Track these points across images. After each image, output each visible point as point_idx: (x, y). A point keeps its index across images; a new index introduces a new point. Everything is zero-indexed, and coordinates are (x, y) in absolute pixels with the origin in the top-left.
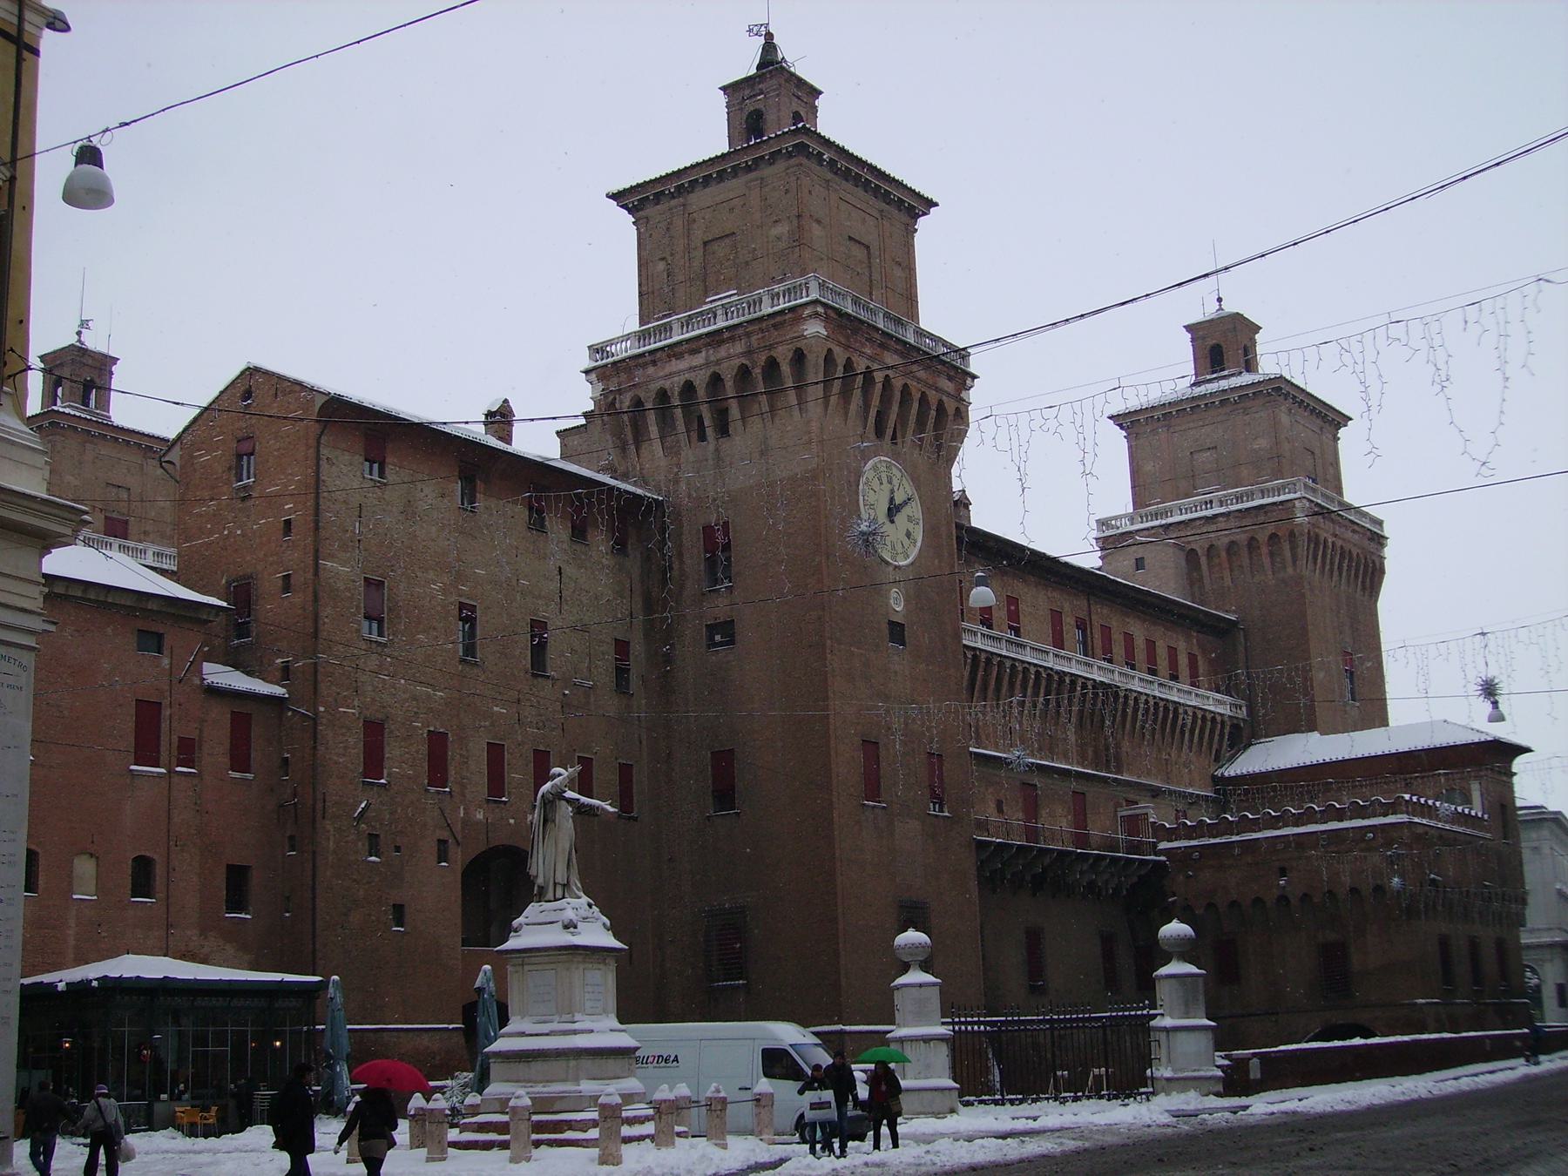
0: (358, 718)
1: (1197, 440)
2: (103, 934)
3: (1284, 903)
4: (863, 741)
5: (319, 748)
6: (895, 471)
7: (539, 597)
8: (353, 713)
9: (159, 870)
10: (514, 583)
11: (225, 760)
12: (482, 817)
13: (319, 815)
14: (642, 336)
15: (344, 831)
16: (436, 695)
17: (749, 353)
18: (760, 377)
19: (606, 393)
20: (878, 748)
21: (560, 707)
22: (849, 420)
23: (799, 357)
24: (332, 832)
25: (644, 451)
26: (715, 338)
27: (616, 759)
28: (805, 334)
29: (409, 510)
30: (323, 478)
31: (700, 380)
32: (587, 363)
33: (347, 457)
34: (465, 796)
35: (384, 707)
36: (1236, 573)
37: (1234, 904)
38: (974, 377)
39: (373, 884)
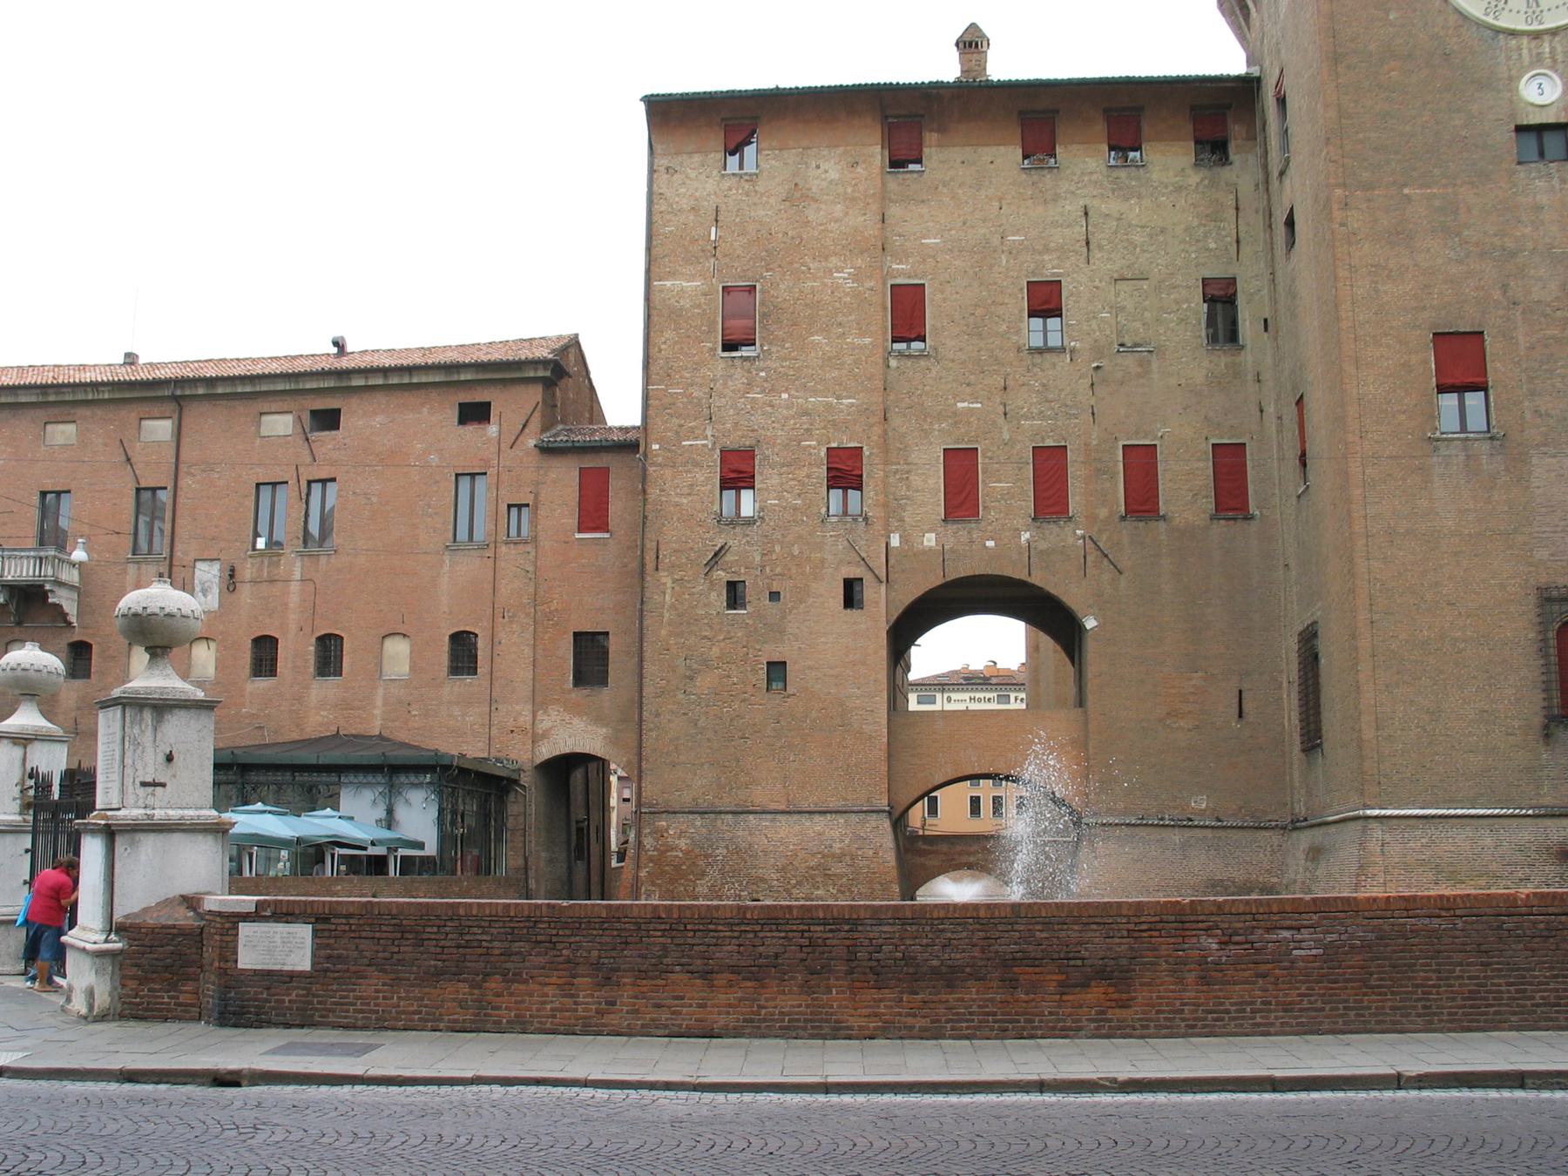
0: (713, 449)
2: (414, 713)
5: (649, 491)
7: (1047, 250)
8: (703, 445)
9: (482, 644)
10: (996, 241)
11: (573, 521)
12: (933, 543)
13: (650, 566)
15: (689, 582)
16: (841, 404)
20: (1483, 341)
24: (669, 584)
25: (1252, 23)
29: (797, 196)
30: (661, 191)
33: (697, 158)
34: (902, 520)
35: (753, 431)
39: (735, 639)
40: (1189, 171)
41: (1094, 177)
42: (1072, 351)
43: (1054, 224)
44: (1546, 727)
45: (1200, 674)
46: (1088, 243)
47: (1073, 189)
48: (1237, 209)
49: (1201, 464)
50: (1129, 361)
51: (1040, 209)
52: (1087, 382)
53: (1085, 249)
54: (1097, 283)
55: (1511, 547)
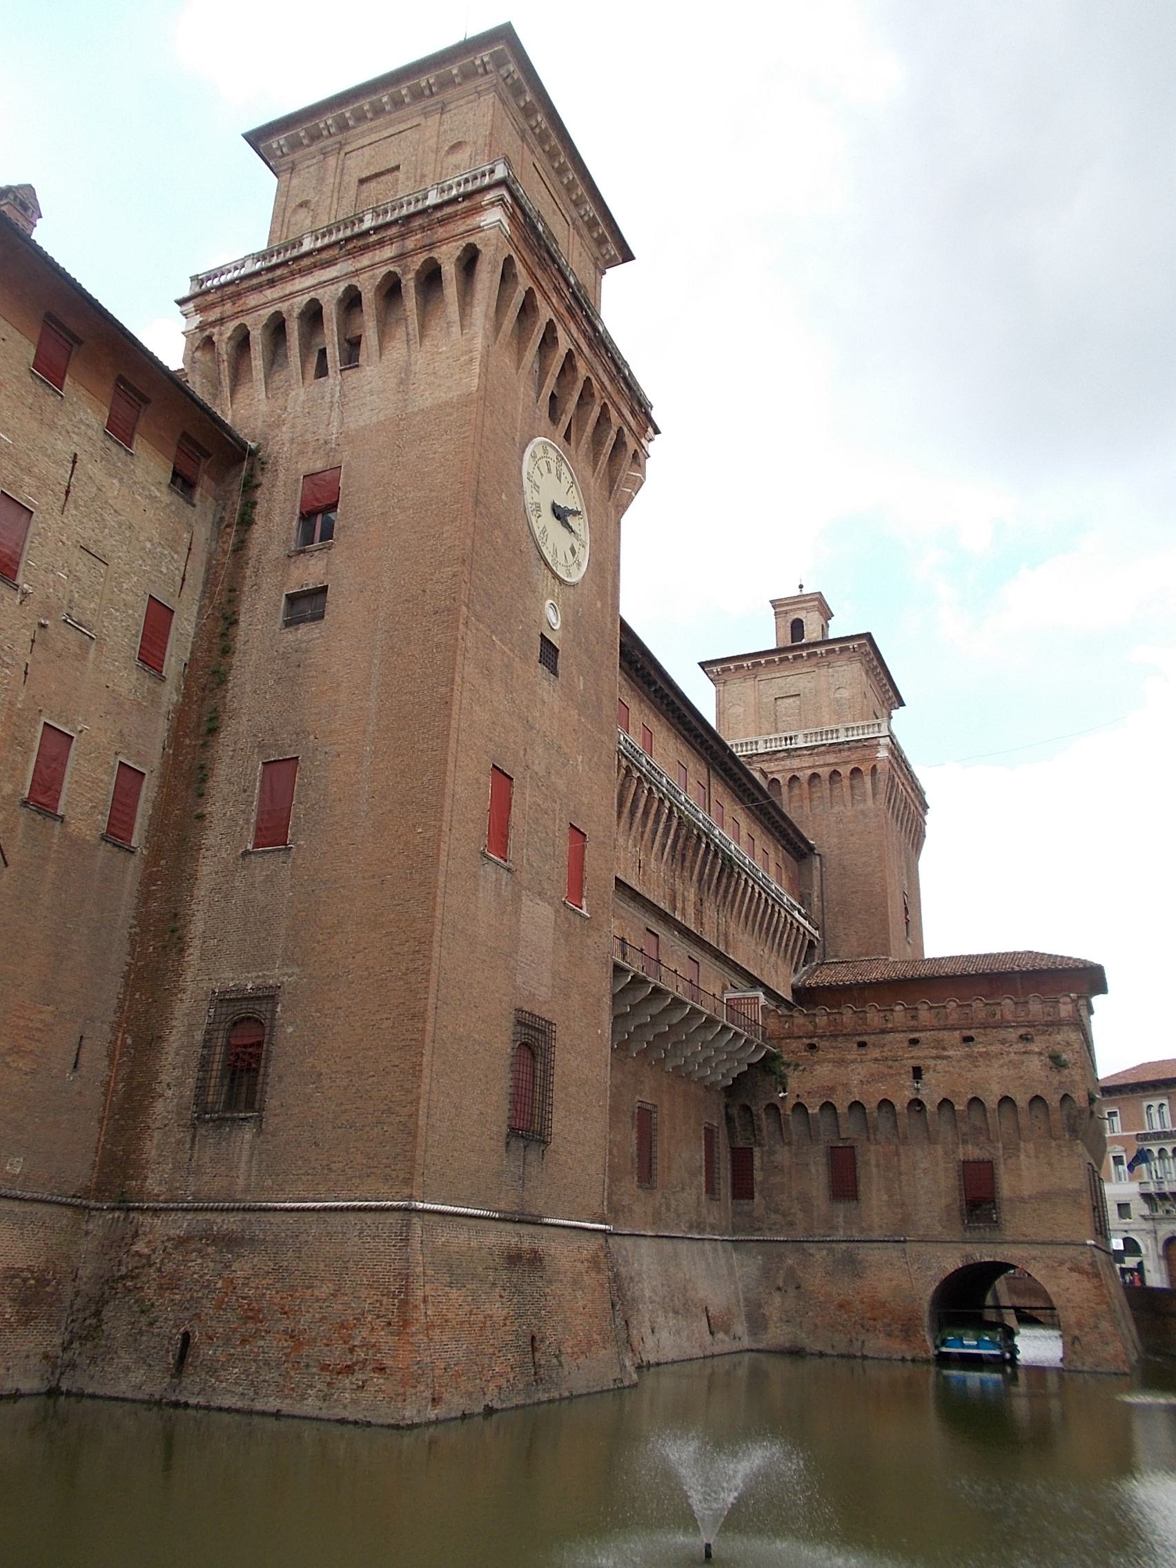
1: (781, 688)
3: (918, 1108)
4: (494, 766)
6: (564, 467)
14: (262, 256)
17: (401, 256)
18: (412, 284)
19: (201, 327)
21: (28, 639)
22: (521, 370)
23: (470, 260)
26: (357, 244)
27: (116, 754)
28: (482, 224)
31: (329, 298)
32: (186, 293)
36: (815, 803)
37: (856, 1105)
38: (657, 431)
40: (164, 489)
41: (90, 432)
42: (25, 594)
43: (43, 450)
44: (508, 1135)
45: (51, 1008)
46: (67, 492)
47: (69, 428)
48: (190, 549)
49: (105, 778)
50: (72, 635)
51: (35, 424)
52: (28, 635)
53: (63, 496)
54: (64, 539)
55: (507, 968)
